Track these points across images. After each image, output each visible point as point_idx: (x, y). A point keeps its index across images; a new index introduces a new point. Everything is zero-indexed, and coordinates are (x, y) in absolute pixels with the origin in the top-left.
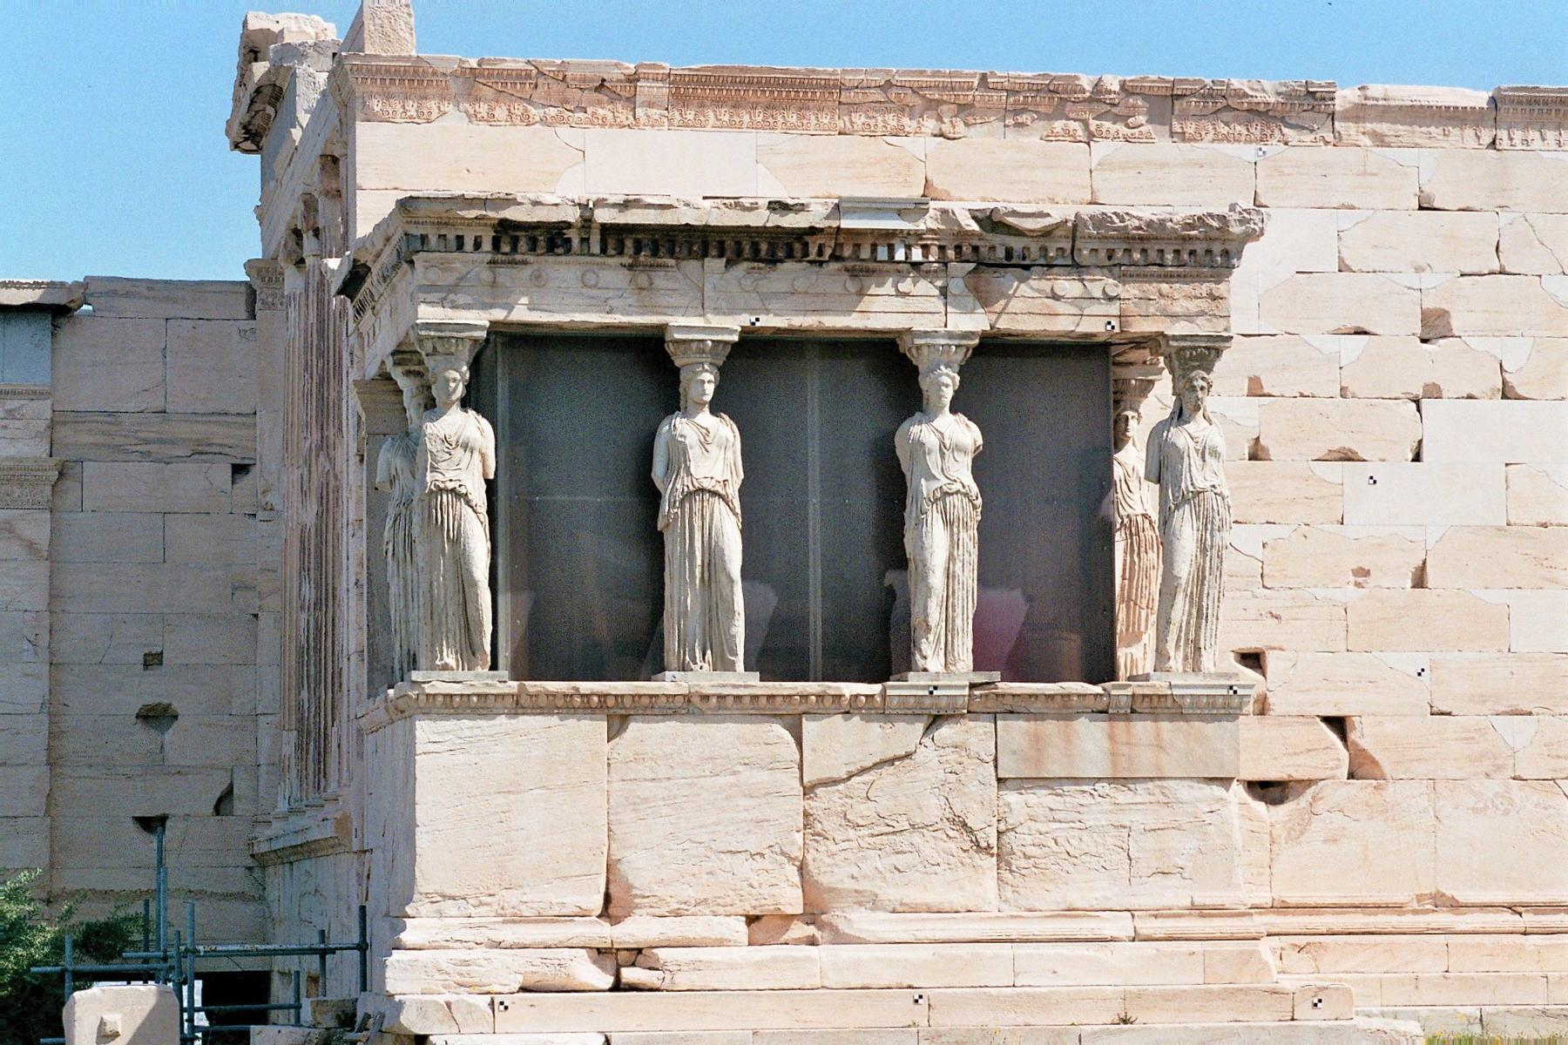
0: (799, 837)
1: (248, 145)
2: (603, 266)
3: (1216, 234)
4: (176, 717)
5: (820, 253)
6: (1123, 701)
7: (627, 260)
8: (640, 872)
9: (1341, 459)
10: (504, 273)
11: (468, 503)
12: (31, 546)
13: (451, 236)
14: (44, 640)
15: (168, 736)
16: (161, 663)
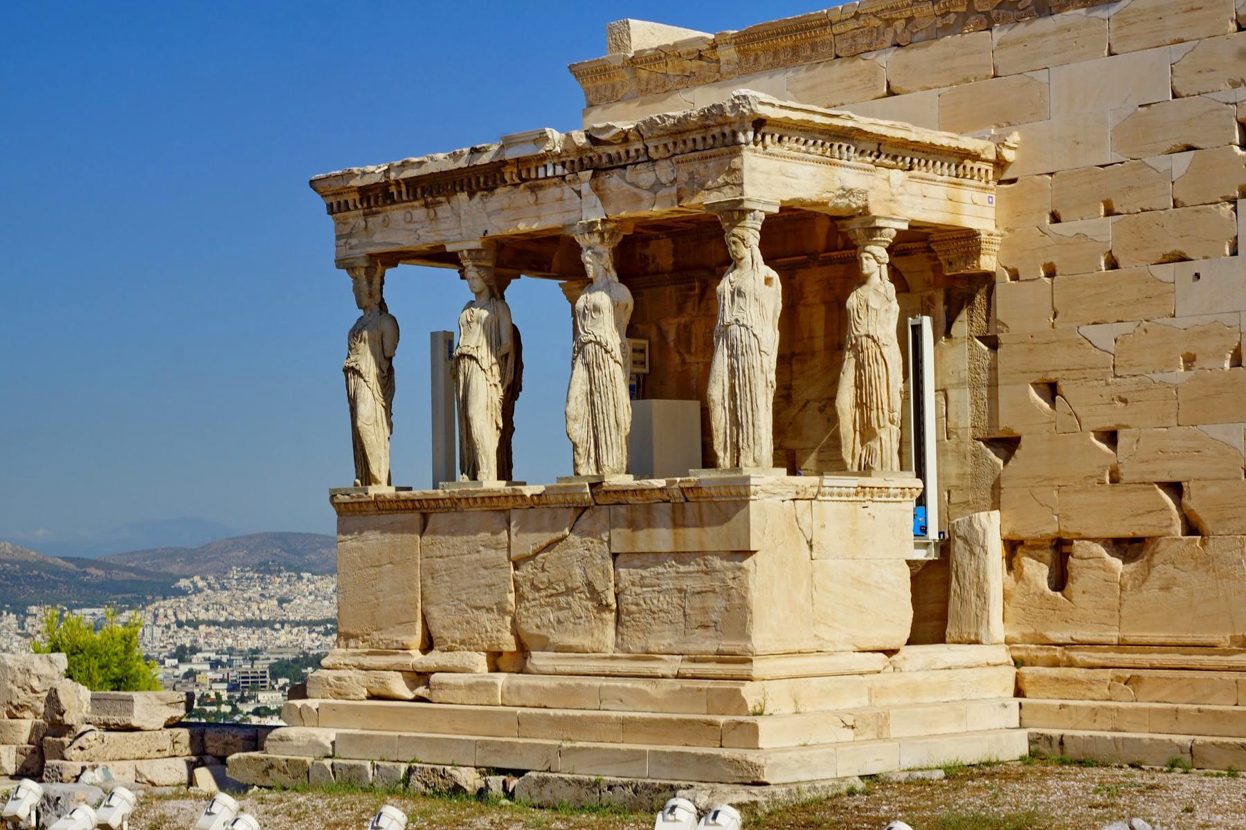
0: (511, 597)
3: (720, 120)
10: (370, 219)
11: (361, 376)
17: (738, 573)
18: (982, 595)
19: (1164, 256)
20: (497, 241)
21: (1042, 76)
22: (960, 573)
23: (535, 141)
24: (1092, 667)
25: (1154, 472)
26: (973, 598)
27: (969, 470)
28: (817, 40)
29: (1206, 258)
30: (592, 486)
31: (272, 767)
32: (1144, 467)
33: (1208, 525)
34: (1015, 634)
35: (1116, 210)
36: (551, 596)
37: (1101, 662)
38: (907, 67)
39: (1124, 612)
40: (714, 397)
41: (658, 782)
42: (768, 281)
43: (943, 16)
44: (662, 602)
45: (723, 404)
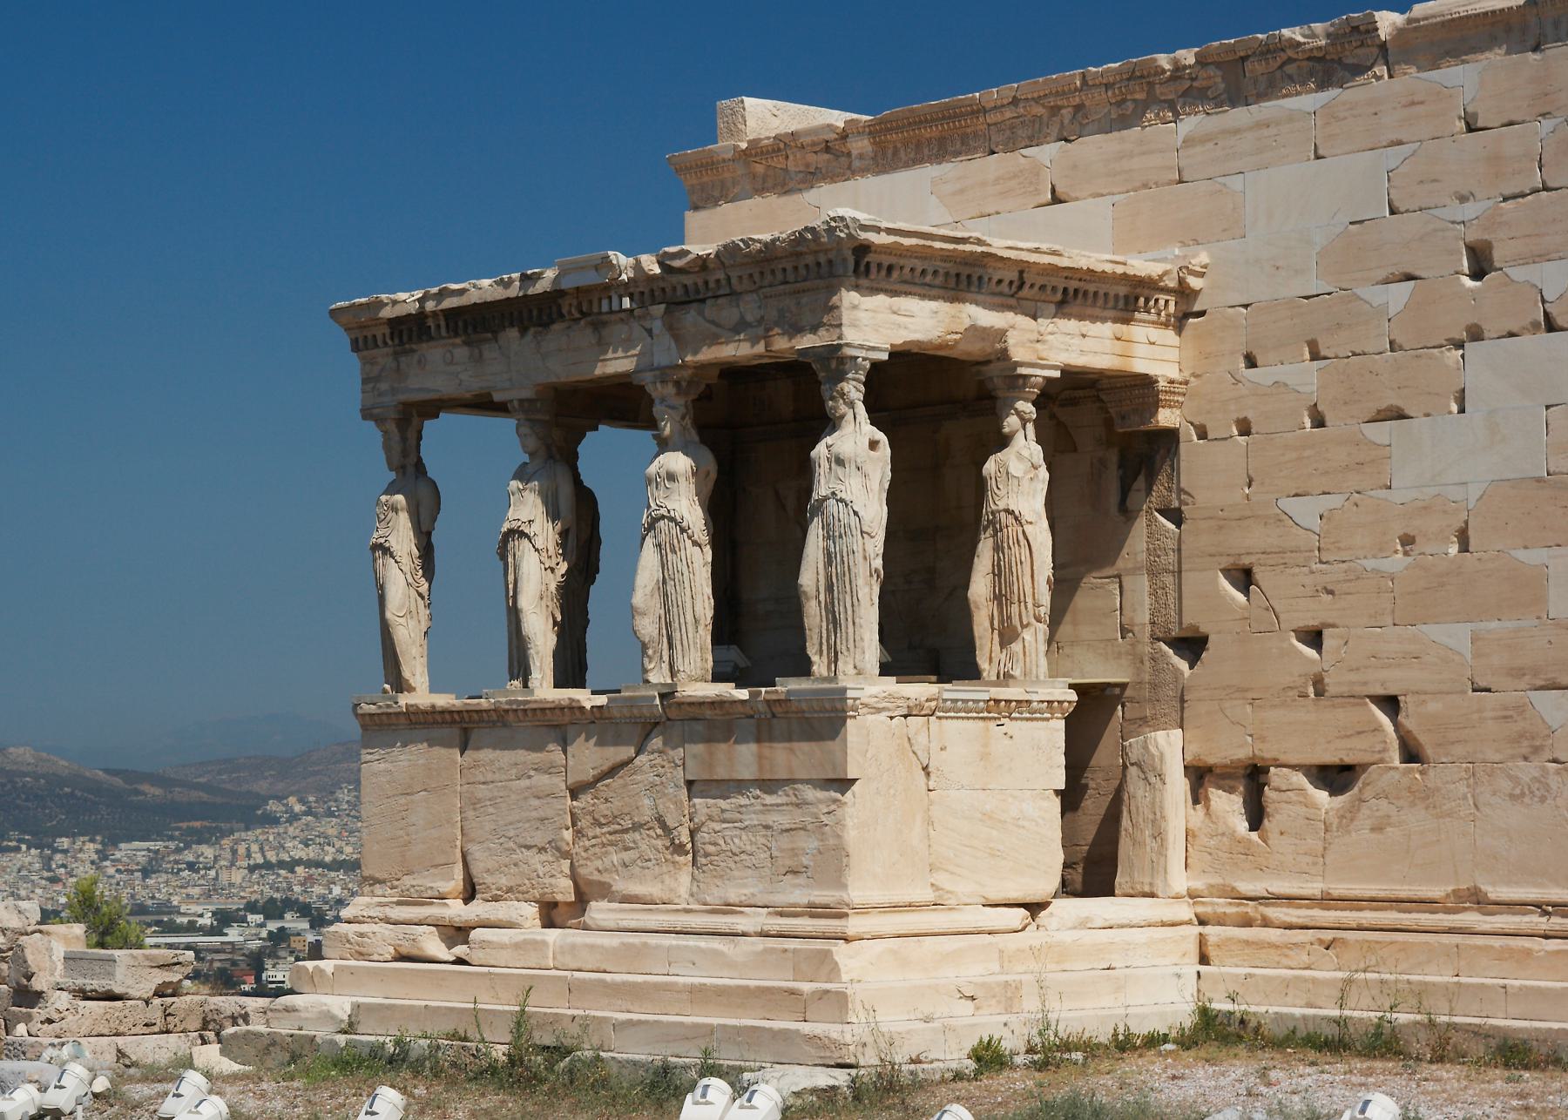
0: (568, 835)
2: (454, 345)
3: (813, 246)
10: (403, 359)
17: (833, 807)
18: (1159, 835)
19: (1379, 412)
20: (556, 389)
21: (1236, 183)
22: (1133, 809)
23: (596, 268)
24: (1290, 927)
25: (1365, 683)
26: (1148, 840)
27: (1147, 678)
29: (1427, 415)
30: (662, 696)
31: (274, 1044)
32: (1353, 677)
33: (1429, 751)
34: (1198, 885)
35: (1323, 353)
36: (615, 832)
37: (1300, 921)
38: (1075, 167)
39: (1328, 860)
40: (805, 588)
42: (873, 445)
44: (742, 841)
45: (817, 597)
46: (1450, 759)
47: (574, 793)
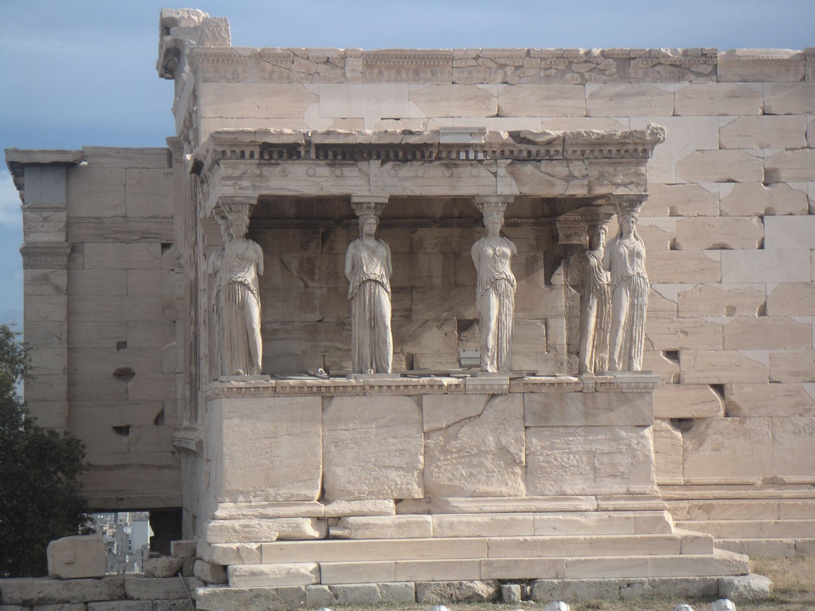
1: (168, 75)
2: (317, 165)
4: (134, 374)
5: (430, 155)
6: (591, 385)
7: (328, 162)
8: (342, 476)
9: (721, 249)
10: (266, 170)
11: (249, 289)
12: (57, 288)
13: (238, 151)
14: (65, 336)
15: (130, 384)
16: (126, 347)
19: (714, 245)
23: (471, 134)
25: (707, 378)
28: (438, 69)
29: (743, 249)
30: (511, 379)
41: (674, 578)
43: (546, 69)
46: (758, 415)
47: (427, 435)
